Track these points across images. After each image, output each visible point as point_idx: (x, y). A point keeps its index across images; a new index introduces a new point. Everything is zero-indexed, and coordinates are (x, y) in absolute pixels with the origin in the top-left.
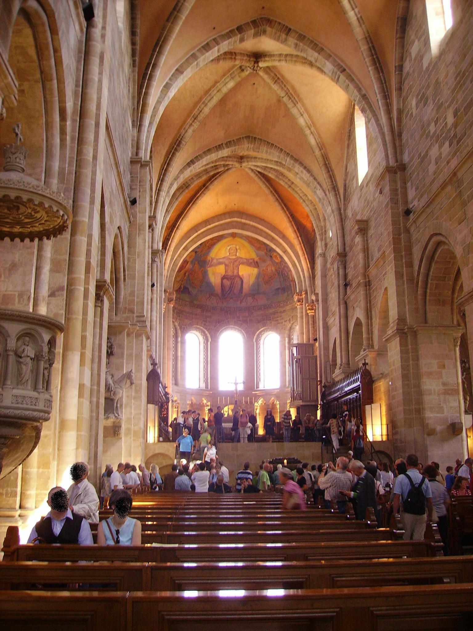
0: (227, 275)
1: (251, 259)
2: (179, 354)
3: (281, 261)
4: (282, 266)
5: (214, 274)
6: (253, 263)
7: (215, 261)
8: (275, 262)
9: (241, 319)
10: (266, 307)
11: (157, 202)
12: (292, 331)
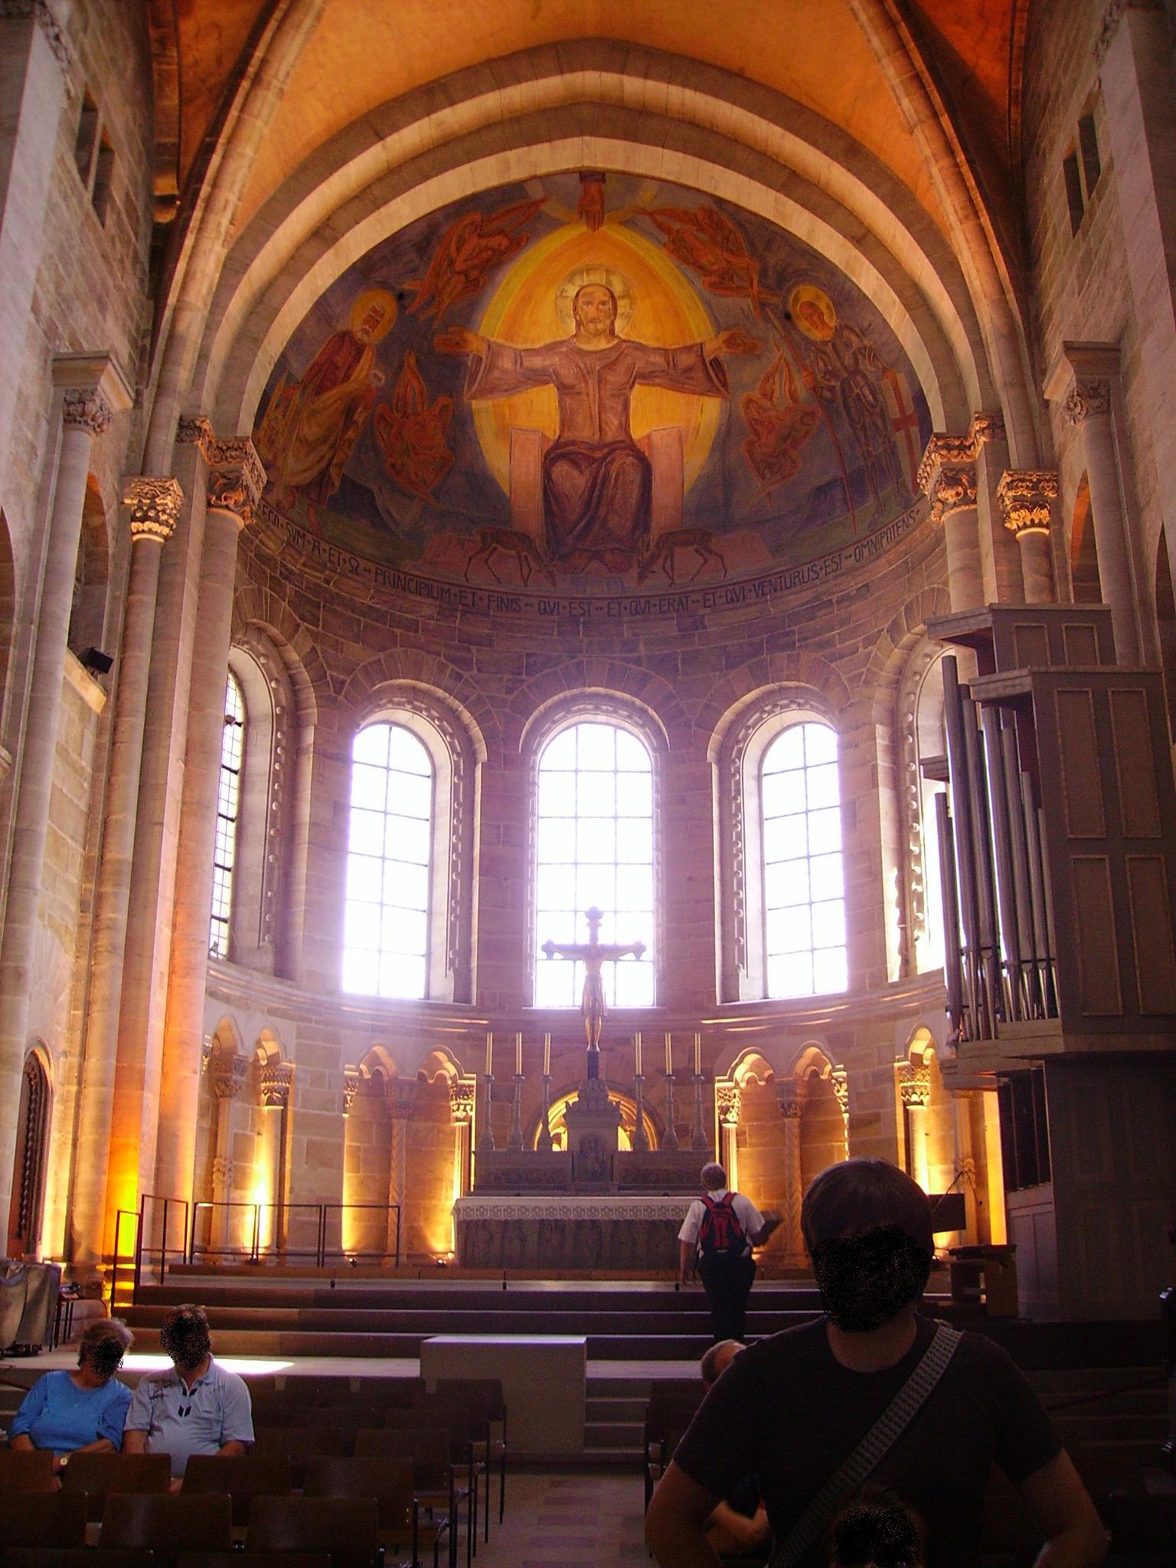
0: (574, 443)
1: (688, 349)
3: (839, 331)
4: (848, 360)
5: (505, 432)
6: (699, 374)
7: (507, 363)
8: (813, 343)
9: (642, 650)
10: (764, 585)
12: (908, 686)
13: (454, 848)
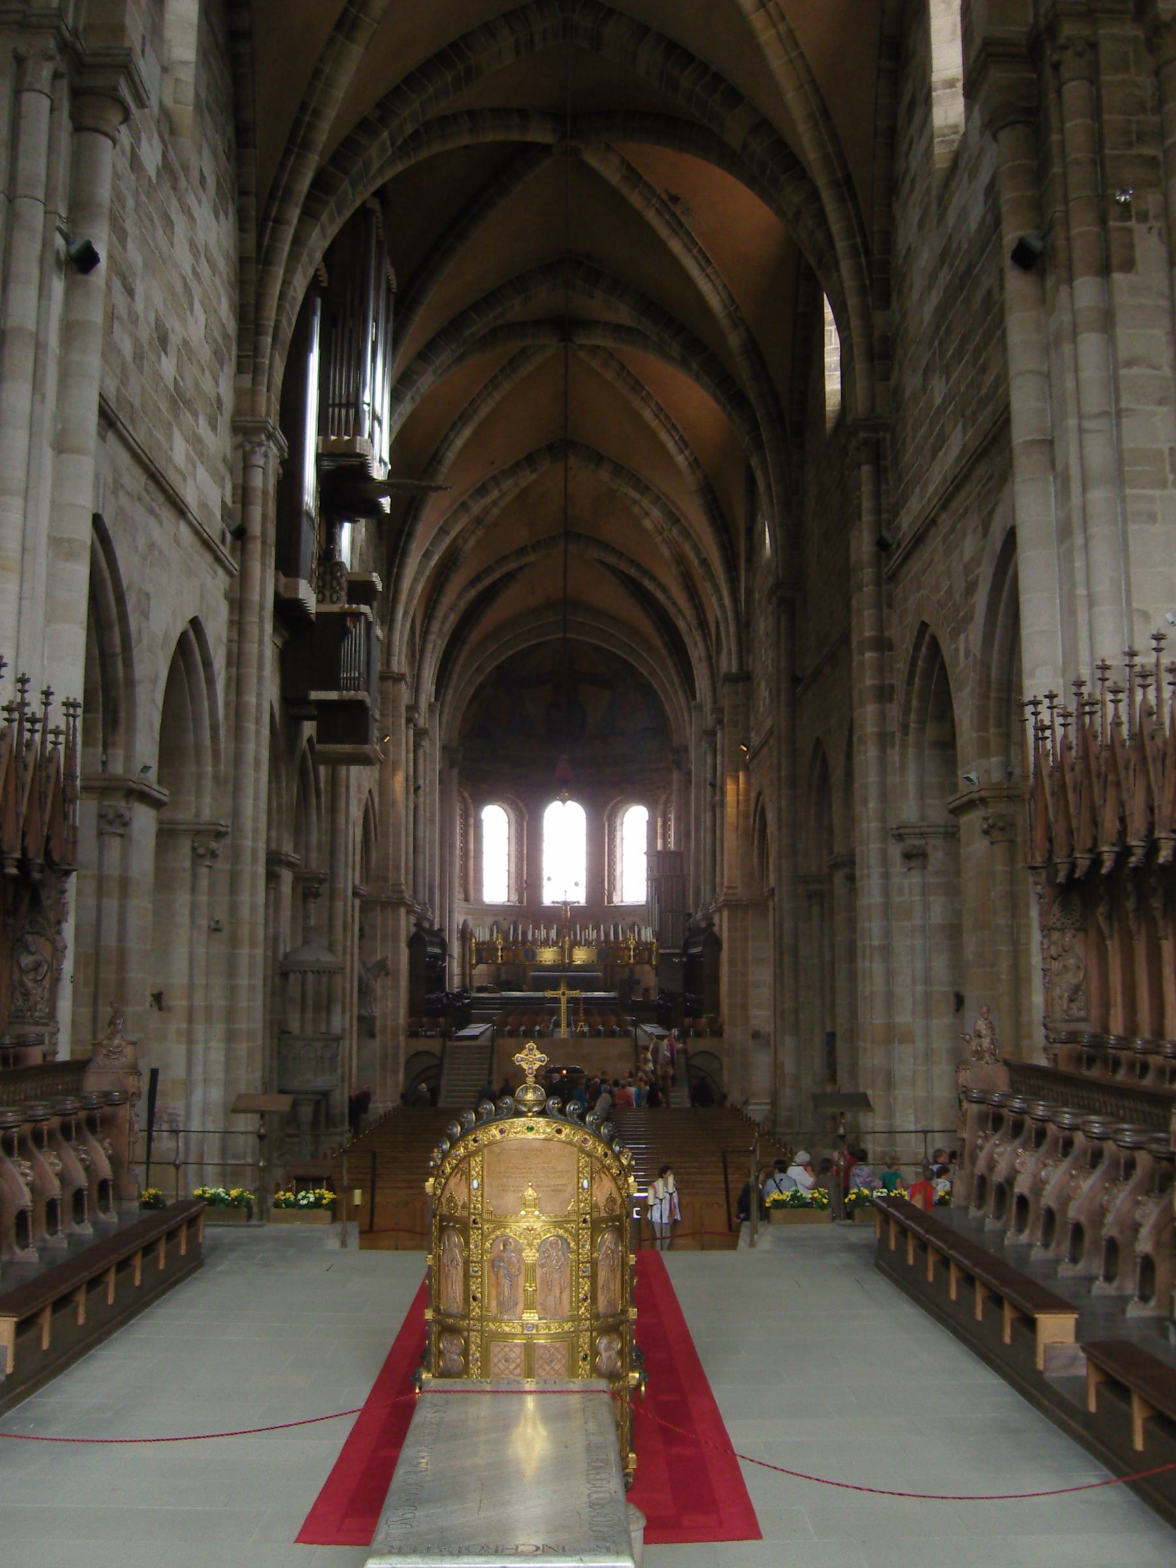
2: (472, 846)
11: (422, 652)
13: (517, 850)
